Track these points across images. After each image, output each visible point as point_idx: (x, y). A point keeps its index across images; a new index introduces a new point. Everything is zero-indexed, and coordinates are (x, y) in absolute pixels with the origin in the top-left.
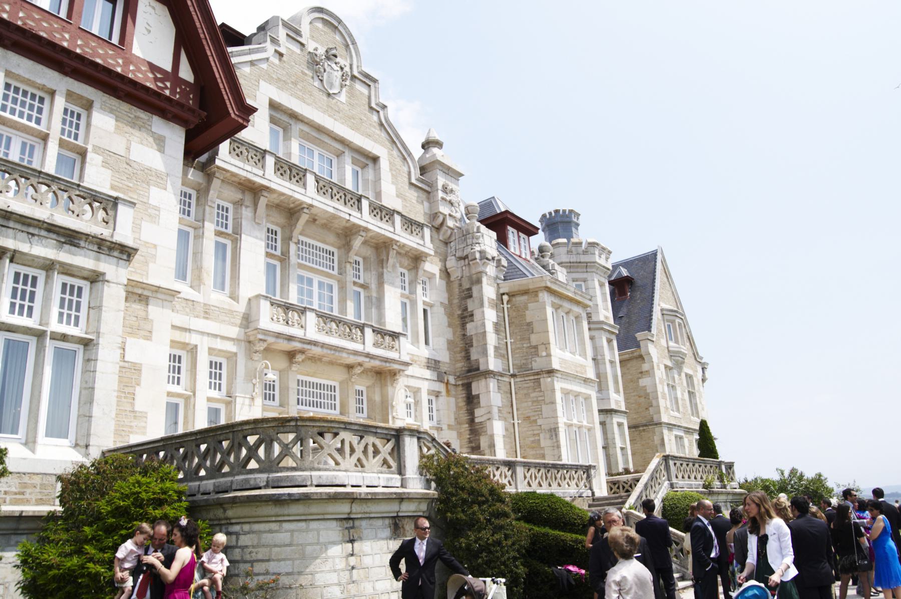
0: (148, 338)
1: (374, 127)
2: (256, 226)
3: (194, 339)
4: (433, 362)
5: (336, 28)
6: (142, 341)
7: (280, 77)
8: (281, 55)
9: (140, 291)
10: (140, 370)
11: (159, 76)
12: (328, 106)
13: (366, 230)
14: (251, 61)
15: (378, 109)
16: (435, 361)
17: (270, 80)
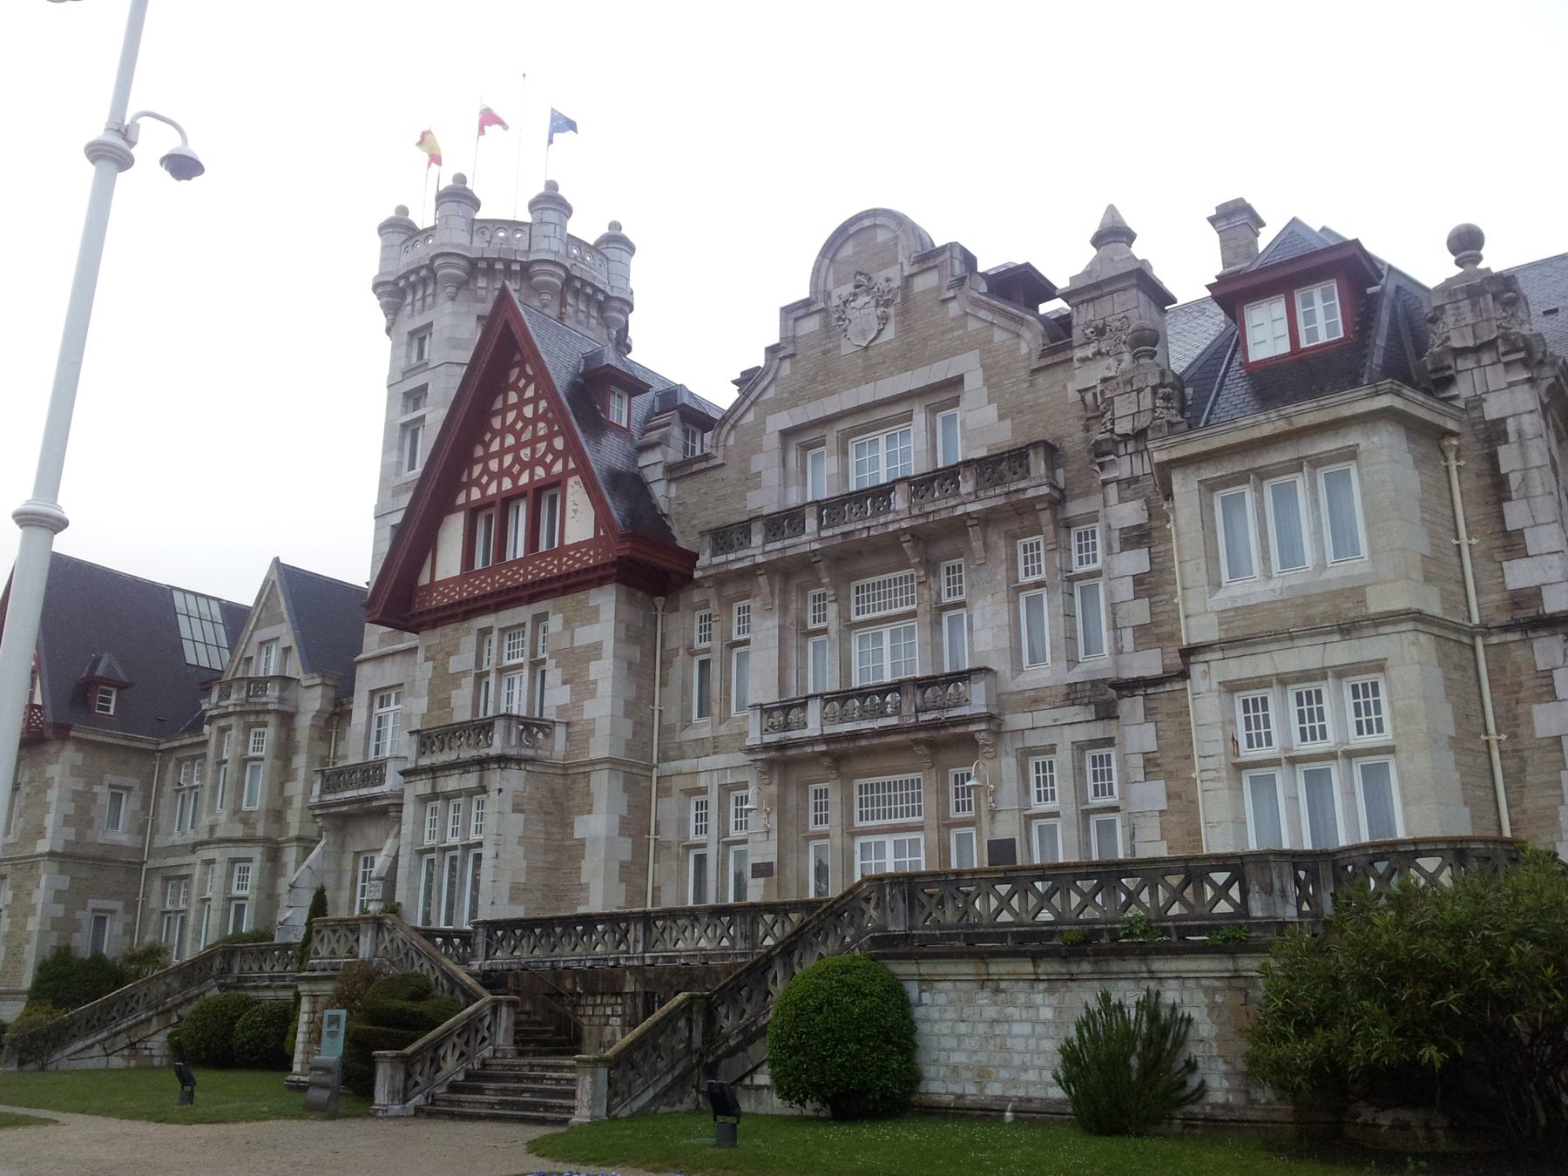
0: (590, 812)
1: (952, 330)
2: (767, 614)
3: (702, 781)
4: (1089, 686)
5: (875, 226)
6: (586, 817)
7: (791, 389)
8: (792, 355)
9: (582, 770)
10: (584, 845)
11: (583, 550)
12: (865, 368)
13: (904, 531)
14: (752, 403)
15: (951, 294)
16: (1094, 683)
17: (780, 405)
